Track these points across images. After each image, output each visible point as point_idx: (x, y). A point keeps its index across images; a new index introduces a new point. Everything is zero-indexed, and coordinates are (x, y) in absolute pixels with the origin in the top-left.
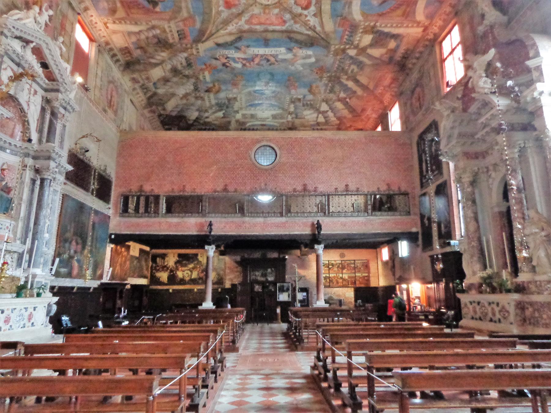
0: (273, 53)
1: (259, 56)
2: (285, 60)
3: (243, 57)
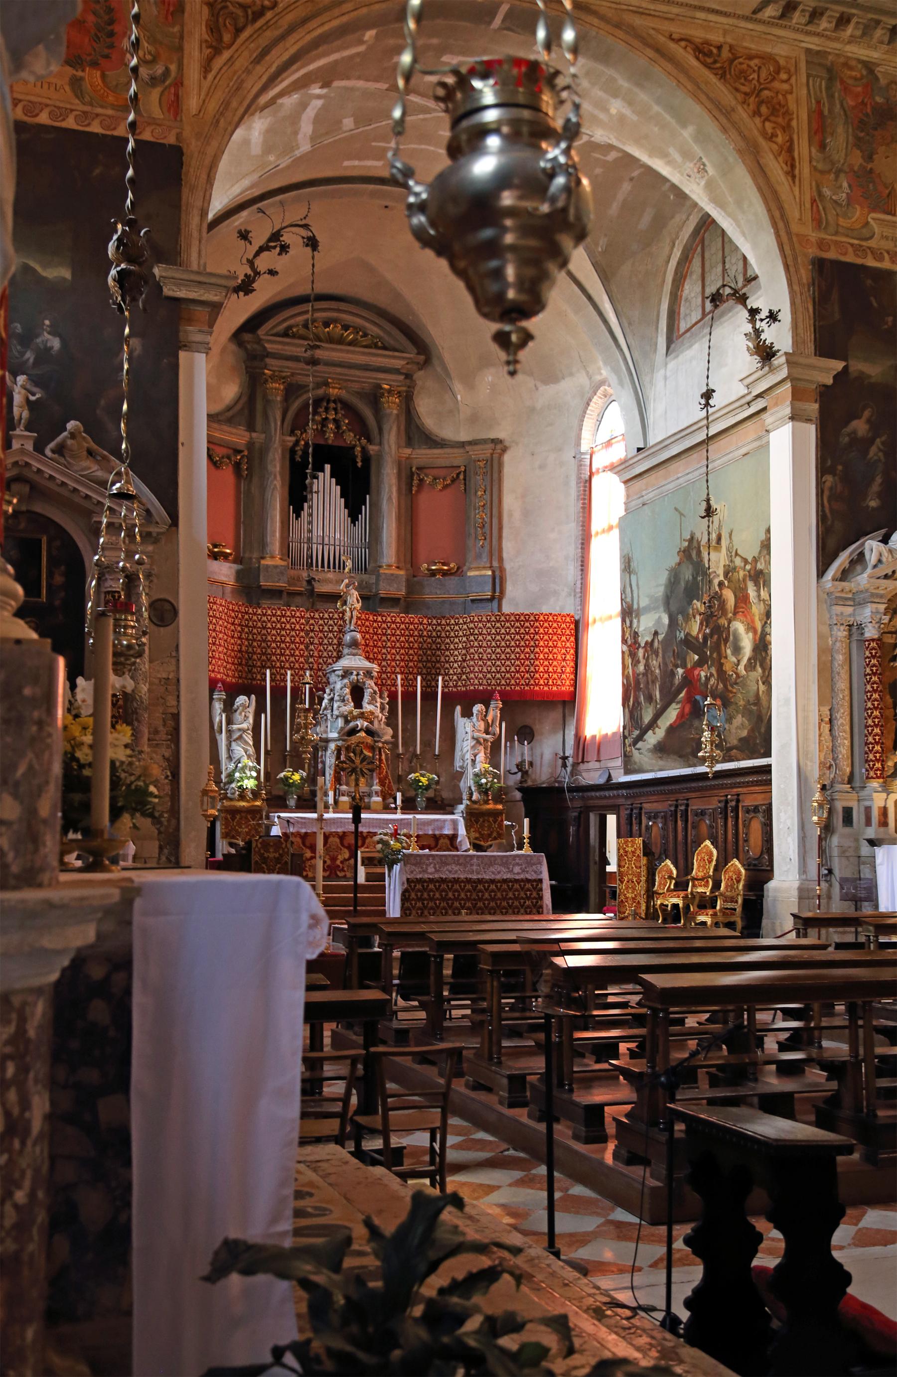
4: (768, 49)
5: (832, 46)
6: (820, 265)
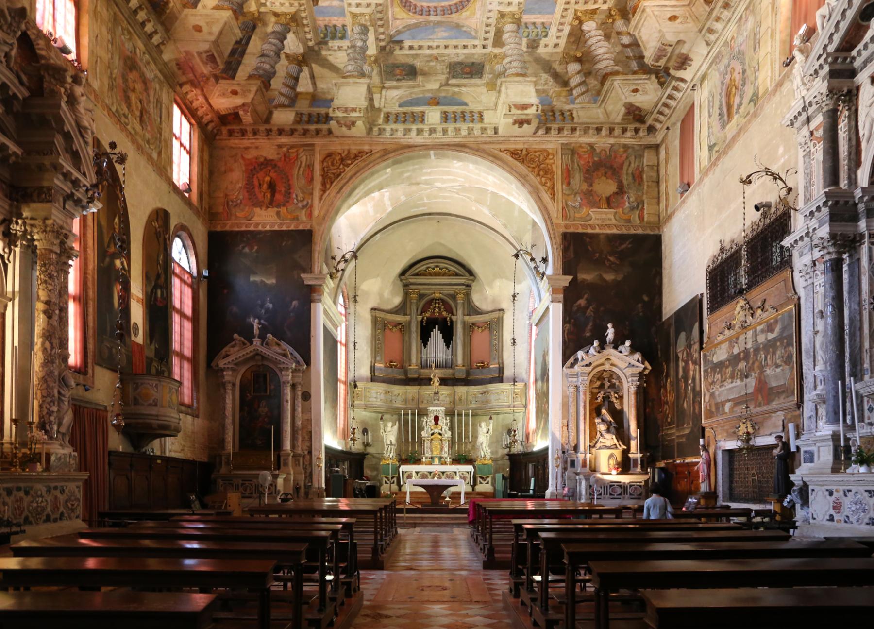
4: (544, 147)
6: (566, 237)
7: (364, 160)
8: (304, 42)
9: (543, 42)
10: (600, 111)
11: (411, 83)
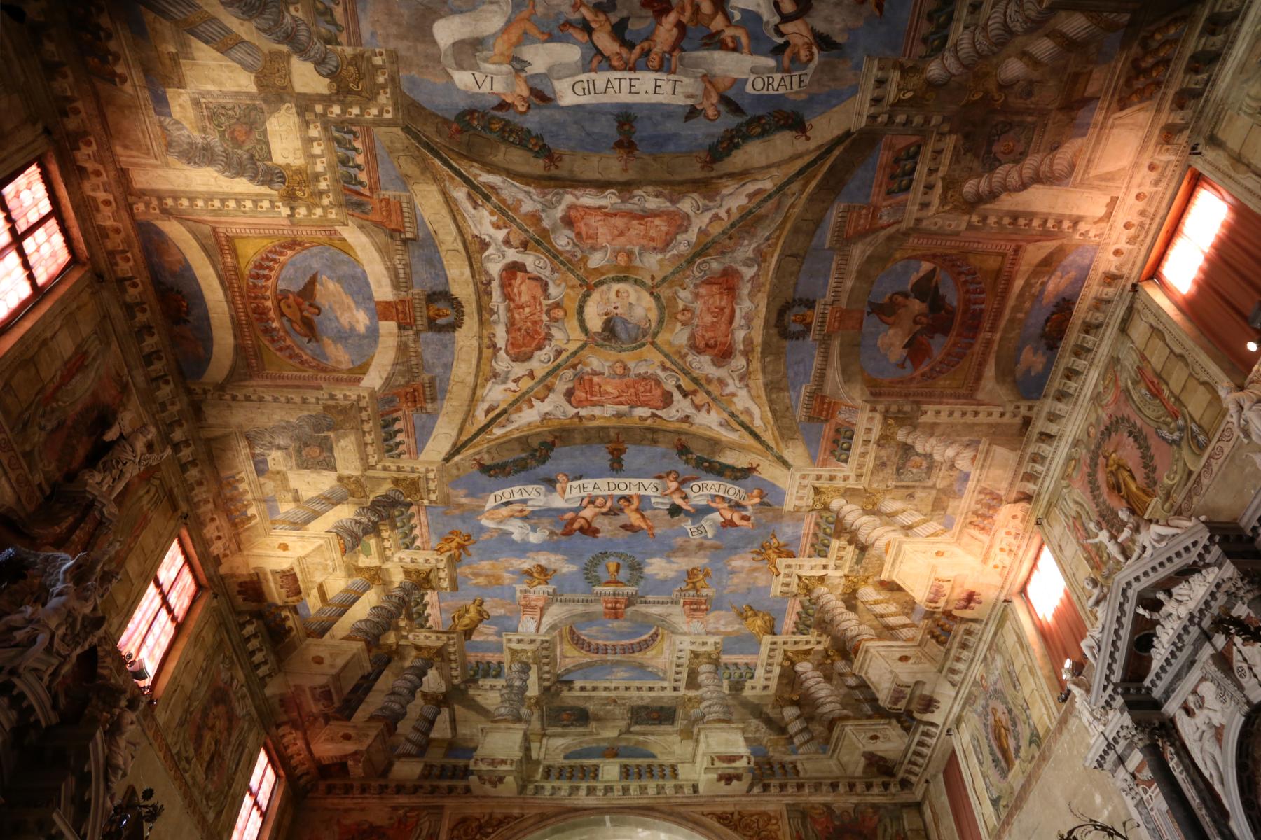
0: (601, 78)
1: (655, 60)
2: (551, 38)
3: (718, 55)
4: (762, 808)
5: (799, 799)
7: (512, 828)
8: (448, 679)
9: (749, 684)
10: (832, 762)
11: (581, 730)
